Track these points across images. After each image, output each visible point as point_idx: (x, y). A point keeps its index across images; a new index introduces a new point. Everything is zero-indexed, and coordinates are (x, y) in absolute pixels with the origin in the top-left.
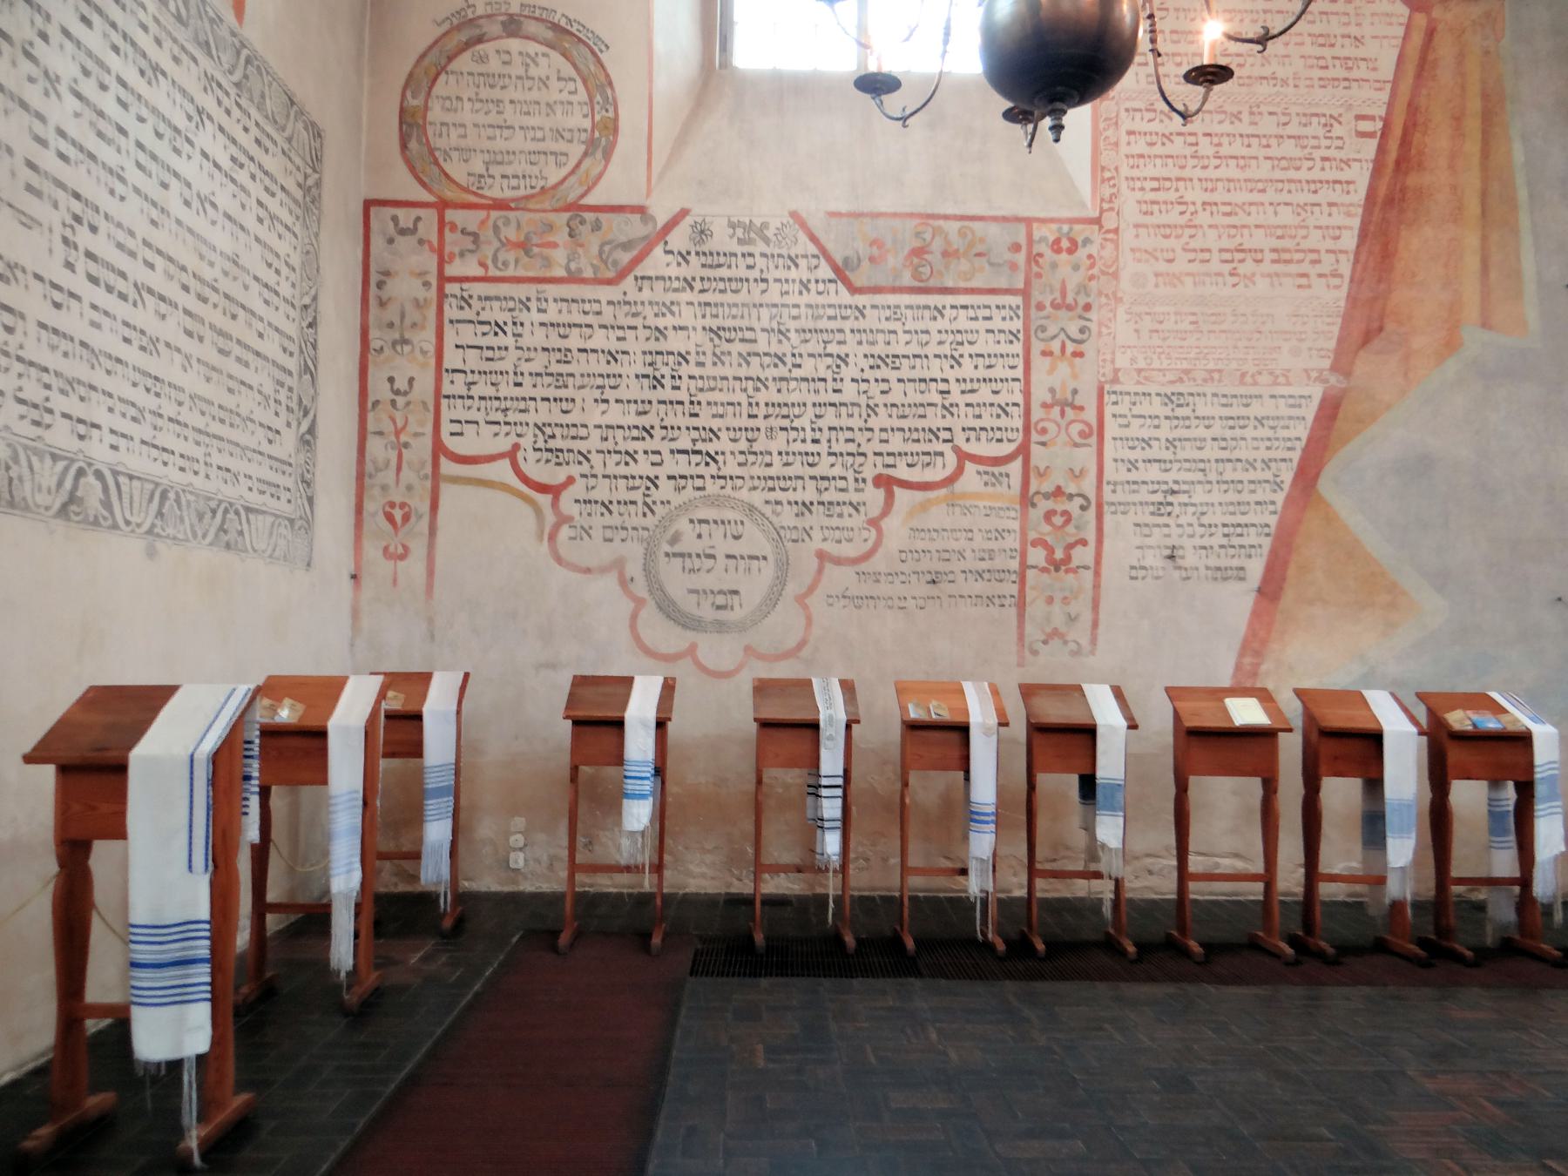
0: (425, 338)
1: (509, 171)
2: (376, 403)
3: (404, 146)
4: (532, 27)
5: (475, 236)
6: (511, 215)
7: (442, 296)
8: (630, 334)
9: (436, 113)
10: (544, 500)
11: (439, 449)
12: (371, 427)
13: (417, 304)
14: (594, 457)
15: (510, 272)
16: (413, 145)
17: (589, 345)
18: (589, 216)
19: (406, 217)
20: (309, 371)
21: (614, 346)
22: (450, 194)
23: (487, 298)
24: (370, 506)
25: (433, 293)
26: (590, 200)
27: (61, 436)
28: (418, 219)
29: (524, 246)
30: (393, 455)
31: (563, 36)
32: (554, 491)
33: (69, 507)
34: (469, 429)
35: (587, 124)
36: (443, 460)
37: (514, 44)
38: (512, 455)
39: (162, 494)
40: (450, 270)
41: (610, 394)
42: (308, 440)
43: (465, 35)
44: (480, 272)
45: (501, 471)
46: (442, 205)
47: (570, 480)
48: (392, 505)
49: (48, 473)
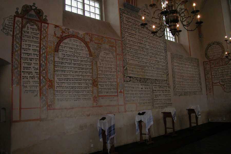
0: (210, 73)
1: (215, 56)
2: (207, 79)
3: (206, 56)
4: (215, 43)
5: (213, 63)
6: (216, 61)
7: (211, 69)
8: (228, 70)
9: (208, 53)
10: (223, 86)
11: (213, 83)
12: (206, 81)
13: (209, 70)
14: (227, 82)
15: (217, 66)
16: (206, 56)
17: (225, 71)
18: (223, 59)
19: (207, 63)
20: (200, 79)
21: (227, 71)
22: (211, 60)
23: (215, 68)
24: (208, 88)
25: (210, 69)
26: (223, 58)
27: (184, 91)
28: (208, 63)
29: (218, 63)
30: (209, 84)
31: (218, 43)
32: (223, 85)
33: (185, 94)
34: (215, 80)
35: (222, 51)
36: (213, 84)
37: (214, 45)
38: (219, 82)
39: (190, 92)
40: (211, 67)
41: (228, 75)
42: (201, 84)
43: (209, 45)
44: (214, 66)
45: (218, 84)
46: (210, 61)
47: (225, 84)
48: (209, 88)
49: (183, 93)
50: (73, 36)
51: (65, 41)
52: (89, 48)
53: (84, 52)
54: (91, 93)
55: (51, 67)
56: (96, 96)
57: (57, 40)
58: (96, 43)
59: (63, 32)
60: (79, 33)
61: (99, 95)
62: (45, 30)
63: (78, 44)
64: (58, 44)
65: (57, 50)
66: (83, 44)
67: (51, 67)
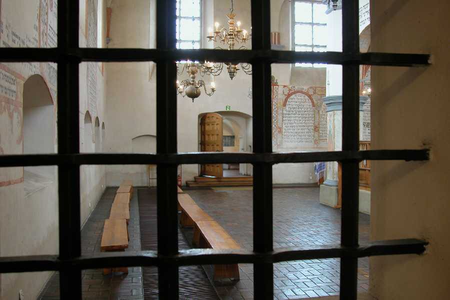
50: (298, 92)
51: (292, 97)
52: (311, 99)
53: (308, 104)
54: (313, 137)
55: (280, 117)
56: (317, 139)
57: (284, 97)
58: (318, 95)
59: (290, 90)
60: (303, 89)
61: (320, 138)
62: (276, 91)
63: (302, 98)
64: (286, 100)
65: (285, 105)
66: (307, 97)
67: (280, 117)
